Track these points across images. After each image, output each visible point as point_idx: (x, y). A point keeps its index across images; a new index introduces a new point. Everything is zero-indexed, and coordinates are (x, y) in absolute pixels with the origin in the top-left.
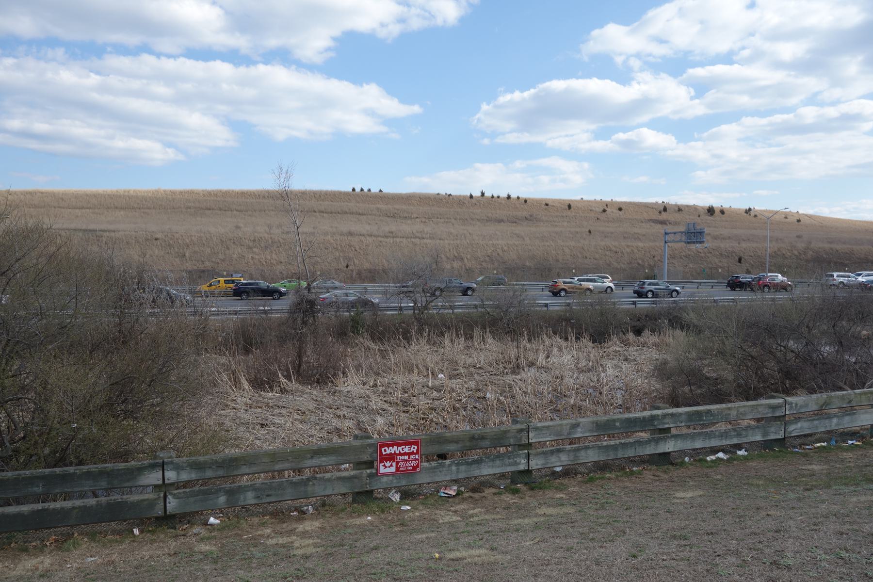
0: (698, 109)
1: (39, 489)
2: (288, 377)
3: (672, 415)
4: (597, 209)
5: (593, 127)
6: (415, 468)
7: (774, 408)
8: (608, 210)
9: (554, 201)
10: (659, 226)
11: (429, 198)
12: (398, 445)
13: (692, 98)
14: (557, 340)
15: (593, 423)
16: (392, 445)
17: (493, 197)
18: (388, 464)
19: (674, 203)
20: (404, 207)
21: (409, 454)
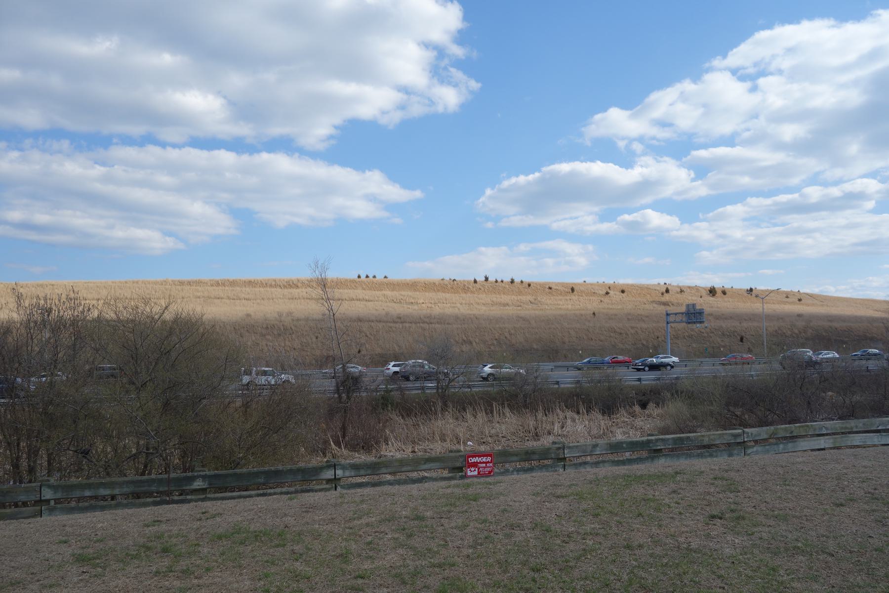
1: (262, 480)
2: (338, 444)
3: (663, 440)
4: (601, 292)
6: (490, 472)
7: (736, 436)
8: (611, 292)
9: (557, 284)
12: (479, 456)
14: (569, 414)
15: (607, 444)
16: (475, 456)
17: (496, 281)
18: (473, 469)
19: (675, 284)
20: (410, 293)
21: (486, 463)
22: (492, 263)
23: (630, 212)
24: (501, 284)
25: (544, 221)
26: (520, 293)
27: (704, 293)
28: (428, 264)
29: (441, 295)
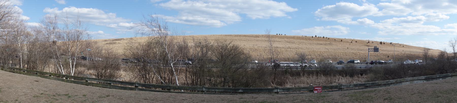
0: (381, 14)
5: (351, 17)
13: (379, 11)
22: (318, 31)
23: (361, 18)
25: (336, 20)
26: (326, 41)
27: (379, 43)
28: (299, 31)
29: (302, 41)
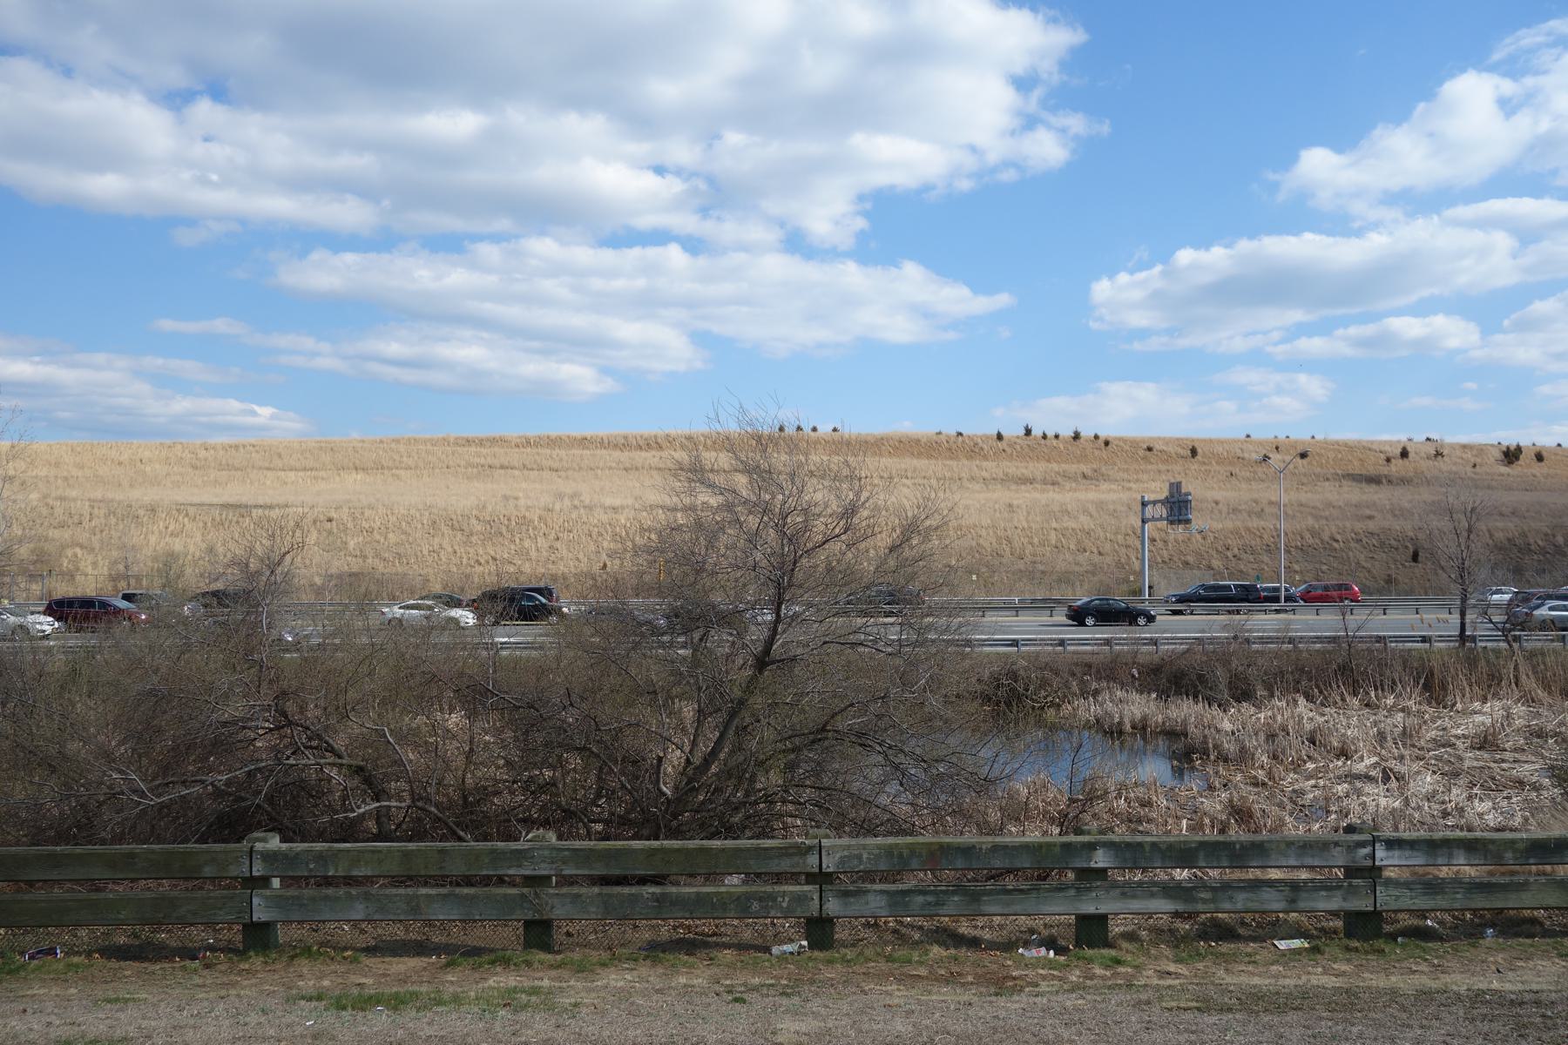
8: (1275, 457)
9: (1167, 441)
10: (1373, 487)
11: (918, 441)
17: (1045, 437)
24: (1055, 442)
